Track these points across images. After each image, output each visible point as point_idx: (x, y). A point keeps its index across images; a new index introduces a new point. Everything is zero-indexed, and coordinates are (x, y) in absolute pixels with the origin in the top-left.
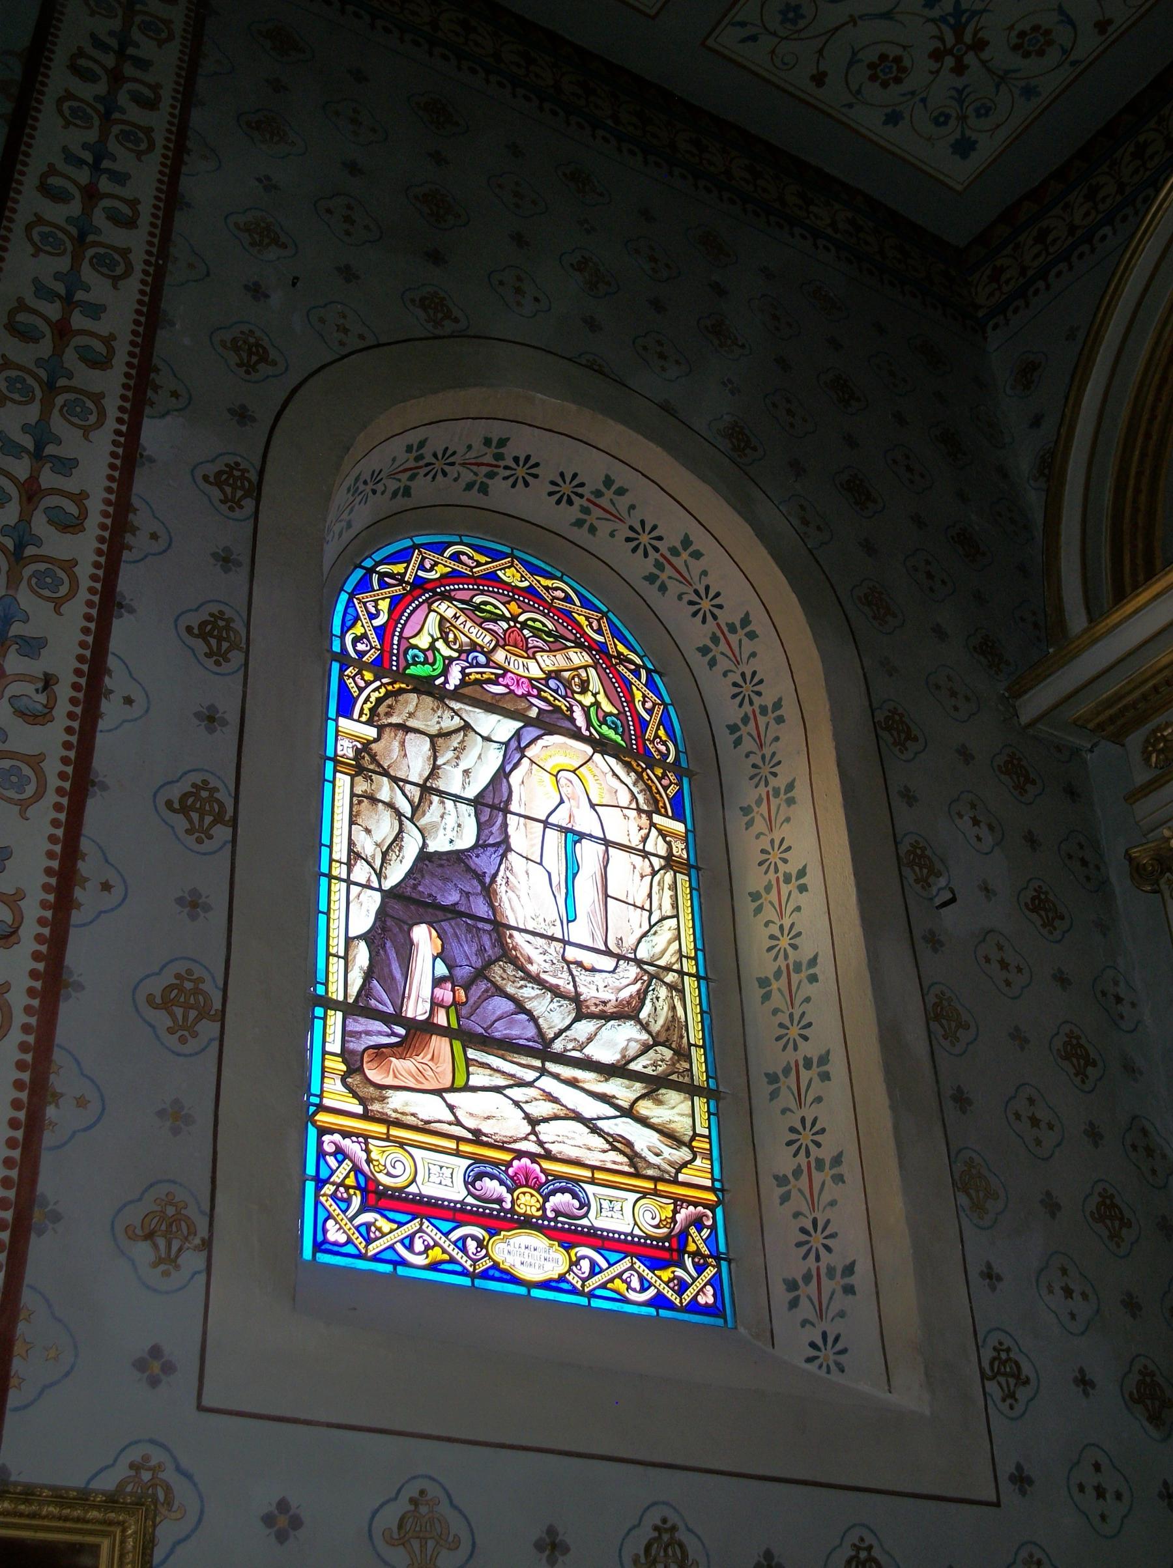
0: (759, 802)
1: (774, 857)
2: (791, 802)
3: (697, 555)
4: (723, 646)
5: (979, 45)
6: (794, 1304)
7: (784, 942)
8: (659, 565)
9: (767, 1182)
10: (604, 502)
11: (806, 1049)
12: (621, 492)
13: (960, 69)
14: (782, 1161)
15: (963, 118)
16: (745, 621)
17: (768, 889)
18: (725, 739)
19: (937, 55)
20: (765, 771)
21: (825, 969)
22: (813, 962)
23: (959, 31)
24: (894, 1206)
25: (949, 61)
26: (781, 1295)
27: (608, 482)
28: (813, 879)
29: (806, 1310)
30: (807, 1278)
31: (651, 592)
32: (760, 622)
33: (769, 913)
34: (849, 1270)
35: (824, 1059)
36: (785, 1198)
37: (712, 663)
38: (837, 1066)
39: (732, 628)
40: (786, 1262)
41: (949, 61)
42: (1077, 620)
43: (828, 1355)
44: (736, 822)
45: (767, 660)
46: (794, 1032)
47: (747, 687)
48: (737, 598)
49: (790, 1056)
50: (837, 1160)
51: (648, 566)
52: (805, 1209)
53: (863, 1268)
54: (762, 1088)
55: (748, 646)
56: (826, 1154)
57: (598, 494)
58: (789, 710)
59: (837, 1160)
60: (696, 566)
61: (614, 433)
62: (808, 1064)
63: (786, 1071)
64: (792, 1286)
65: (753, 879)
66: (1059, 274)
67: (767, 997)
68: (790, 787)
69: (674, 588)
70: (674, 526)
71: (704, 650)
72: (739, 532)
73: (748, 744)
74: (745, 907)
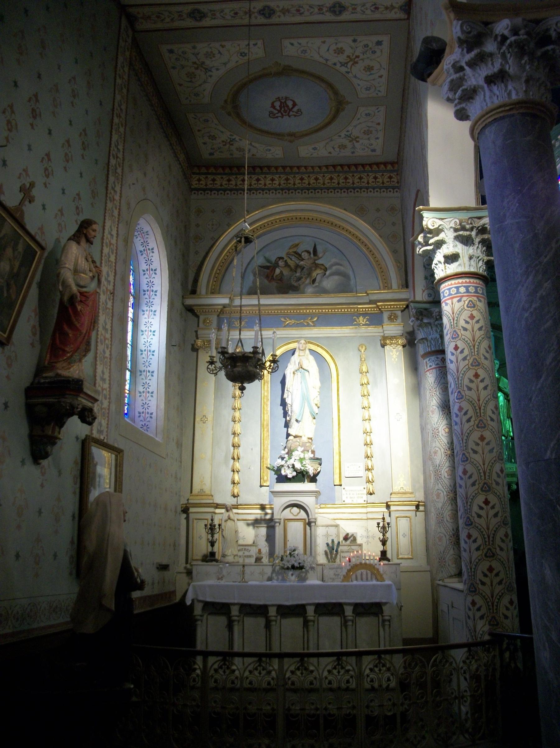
0: (147, 311)
1: (148, 325)
2: (155, 315)
3: (153, 252)
4: (148, 272)
5: (232, 145)
6: (139, 416)
7: (148, 344)
8: (144, 250)
9: (137, 392)
10: (143, 235)
11: (149, 369)
12: (148, 234)
13: (225, 145)
14: (141, 389)
15: (216, 151)
16: (155, 270)
17: (146, 331)
18: (142, 293)
19: (223, 141)
20: (150, 304)
21: (156, 354)
22: (154, 351)
23: (231, 141)
24: (162, 406)
25: (224, 143)
26: (137, 414)
27: (147, 232)
28: (157, 334)
29: (141, 418)
30: (143, 413)
31: (139, 254)
32: (158, 272)
33: (144, 336)
34: (152, 414)
35: (153, 372)
36: (140, 396)
37: (144, 274)
38: (155, 374)
39: (152, 270)
40: (139, 409)
41: (224, 143)
42: (204, 291)
43: (145, 428)
44: (141, 313)
45: (157, 281)
46: (147, 364)
47: (151, 284)
48: (156, 264)
49: (145, 368)
50: (152, 393)
51: (142, 249)
52: (144, 399)
53: (154, 414)
54: (139, 373)
55: (154, 275)
56: (150, 390)
57: (143, 233)
58: (158, 294)
59: (152, 393)
60: (151, 254)
61: (156, 226)
62: (149, 372)
63: (144, 371)
64: (139, 413)
65: (142, 327)
66: (215, 193)
67: (142, 354)
68: (155, 311)
69: (144, 255)
70: (152, 244)
71: (144, 271)
72: (164, 253)
73: (146, 296)
74: (140, 333)
